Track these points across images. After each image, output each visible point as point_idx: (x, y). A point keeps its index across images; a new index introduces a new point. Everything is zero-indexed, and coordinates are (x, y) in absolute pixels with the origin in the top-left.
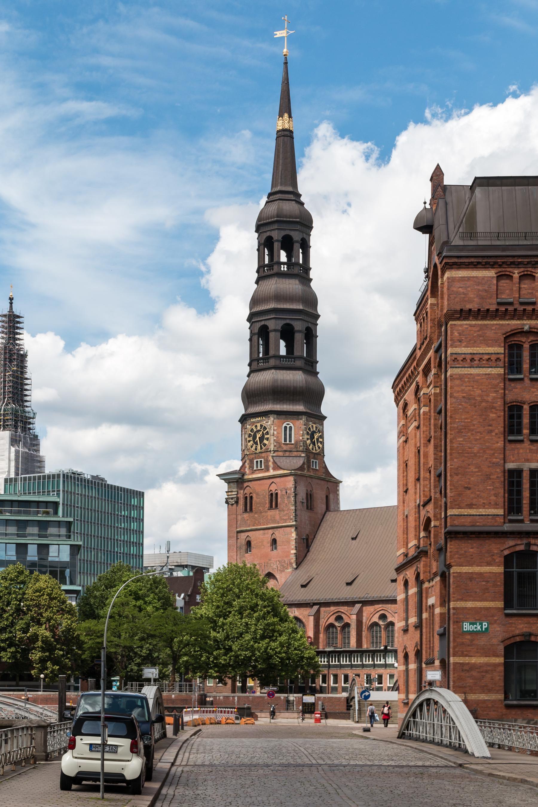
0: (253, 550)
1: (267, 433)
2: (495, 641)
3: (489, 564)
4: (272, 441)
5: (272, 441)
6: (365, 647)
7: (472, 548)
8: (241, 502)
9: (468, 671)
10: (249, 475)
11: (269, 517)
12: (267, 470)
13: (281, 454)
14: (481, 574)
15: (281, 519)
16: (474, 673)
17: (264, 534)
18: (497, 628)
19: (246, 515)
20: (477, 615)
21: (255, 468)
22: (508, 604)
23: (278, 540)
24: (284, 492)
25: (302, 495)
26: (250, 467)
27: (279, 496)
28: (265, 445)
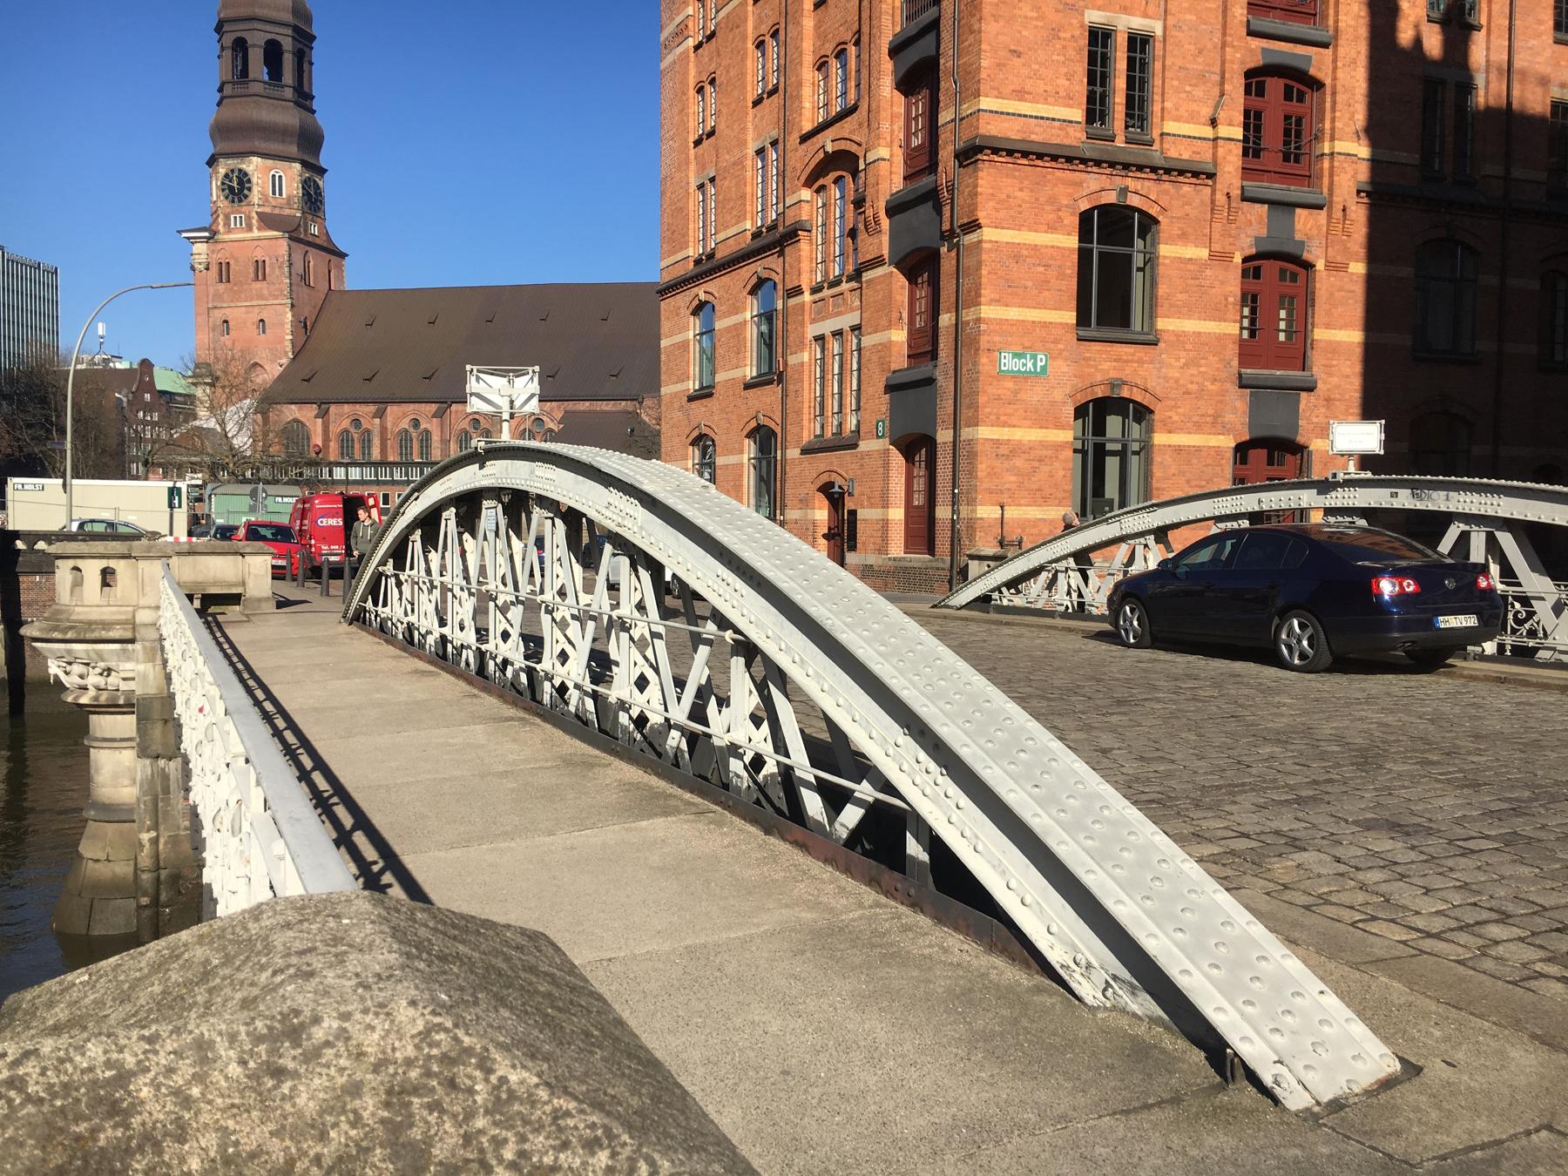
1: (249, 181)
2: (1058, 395)
3: (1051, 228)
6: (391, 459)
7: (1021, 190)
9: (1007, 457)
12: (250, 228)
13: (268, 210)
14: (1035, 248)
16: (1019, 462)
18: (1062, 367)
19: (221, 287)
20: (1029, 338)
22: (1083, 320)
25: (298, 267)
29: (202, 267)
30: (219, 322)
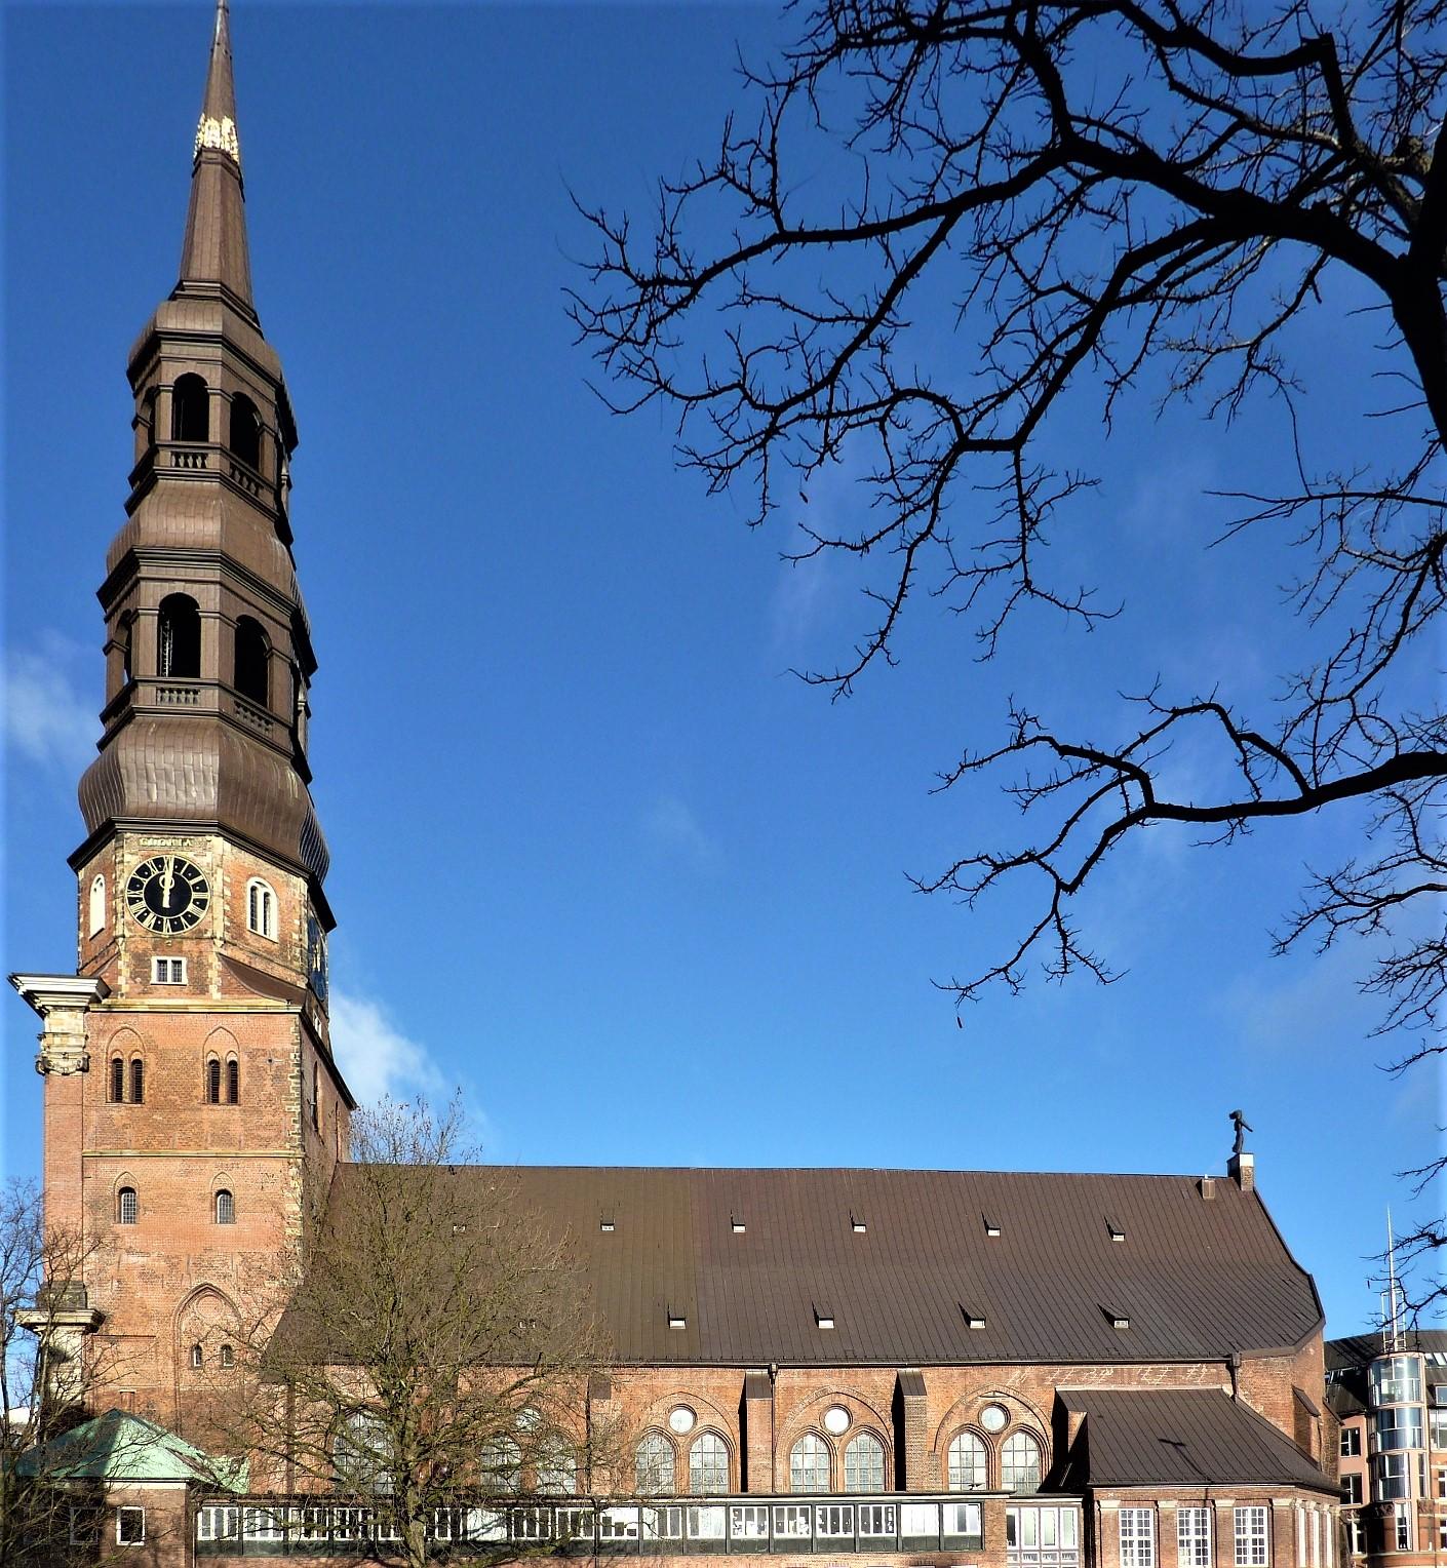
0: (145, 1217)
4: (218, 913)
5: (218, 913)
8: (102, 1074)
10: (128, 995)
11: (206, 1127)
15: (251, 1136)
17: (188, 1173)
19: (119, 1113)
21: (154, 979)
23: (237, 1193)
24: (261, 1061)
26: (134, 976)
27: (243, 1071)
28: (192, 919)
29: (70, 1065)
30: (111, 1191)
